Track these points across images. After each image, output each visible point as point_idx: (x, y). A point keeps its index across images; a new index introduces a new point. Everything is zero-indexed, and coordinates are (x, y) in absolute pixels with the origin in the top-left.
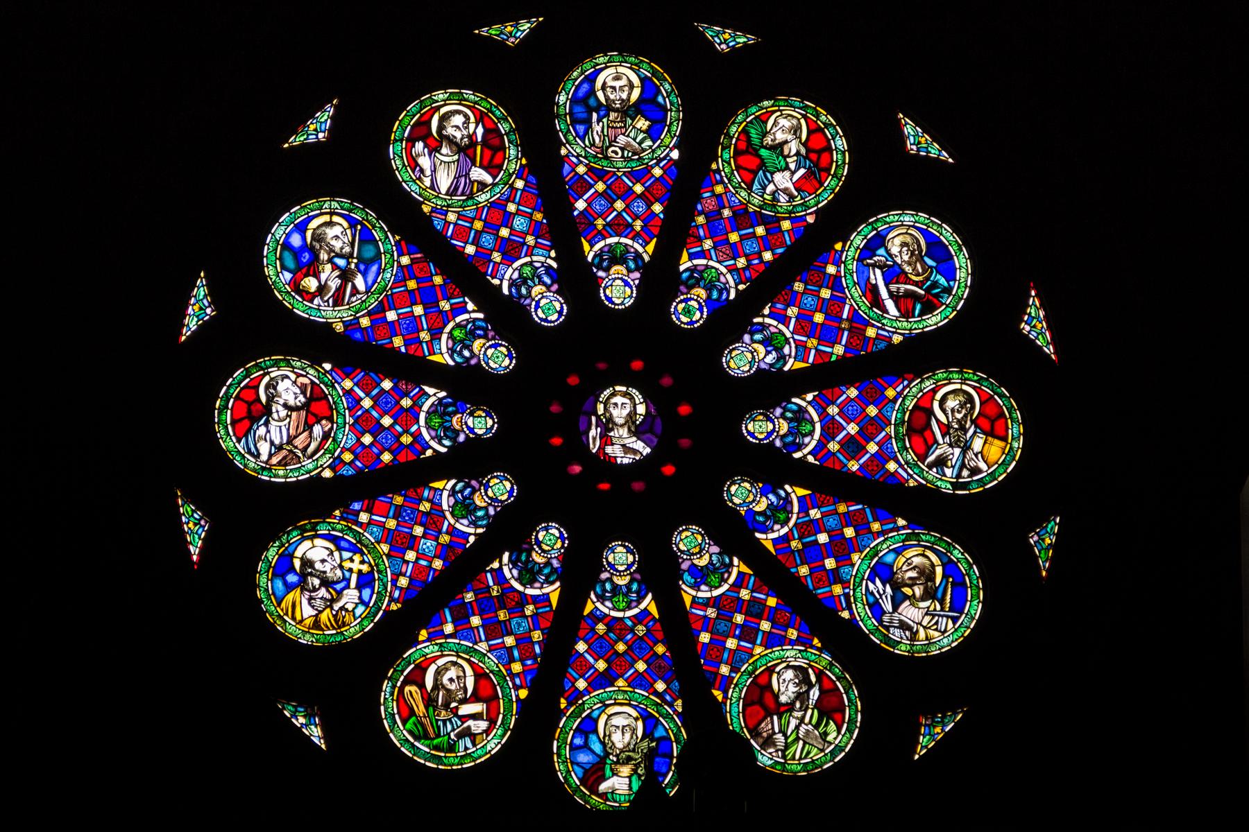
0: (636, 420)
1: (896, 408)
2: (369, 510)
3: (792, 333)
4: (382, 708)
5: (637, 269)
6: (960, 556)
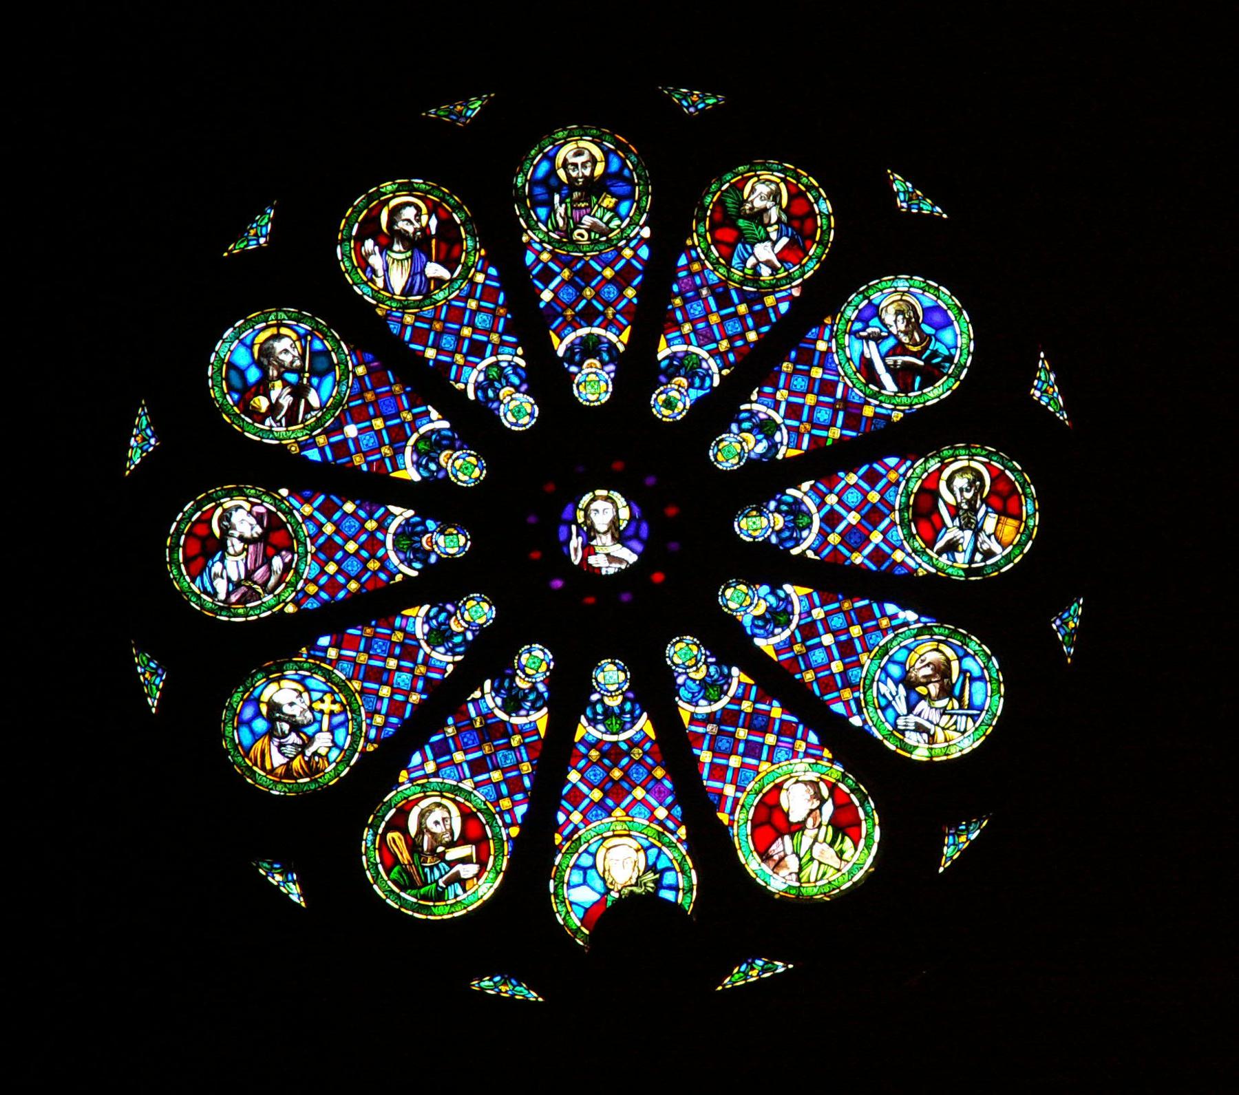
1: (900, 492)
2: (336, 644)
3: (783, 418)
4: (364, 858)
5: (611, 362)
6: (977, 648)
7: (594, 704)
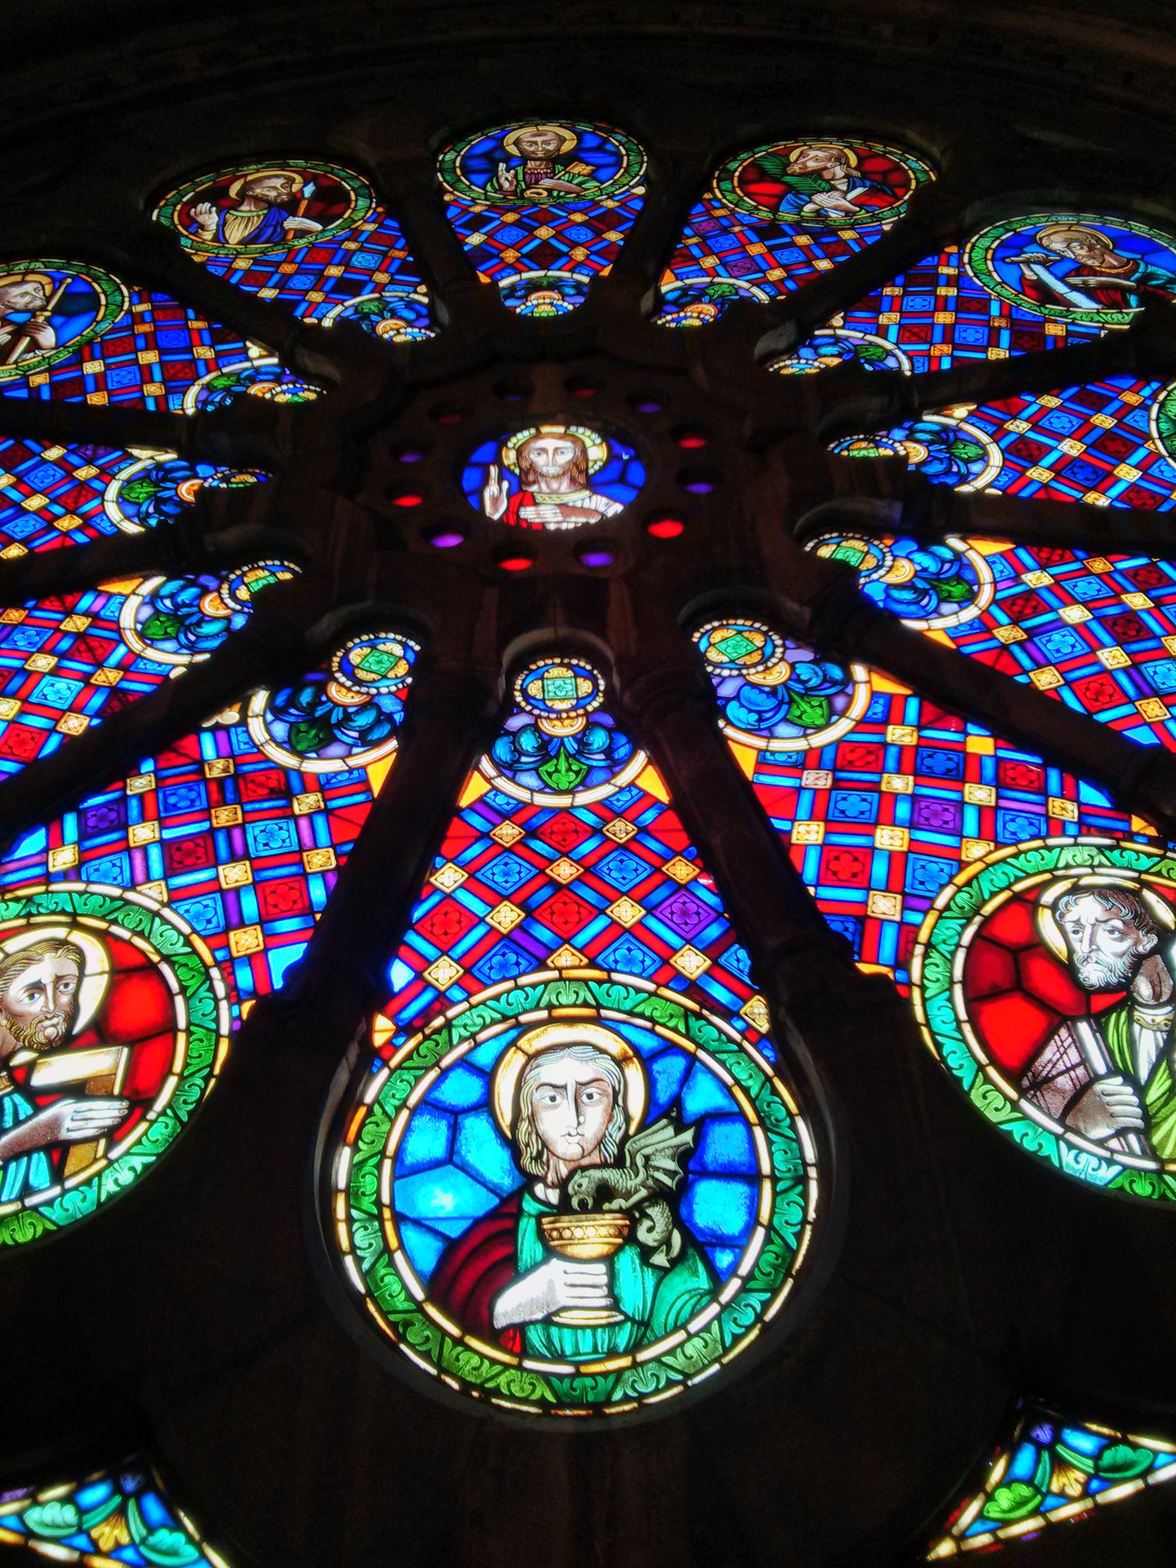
0: (587, 468)
7: (515, 735)
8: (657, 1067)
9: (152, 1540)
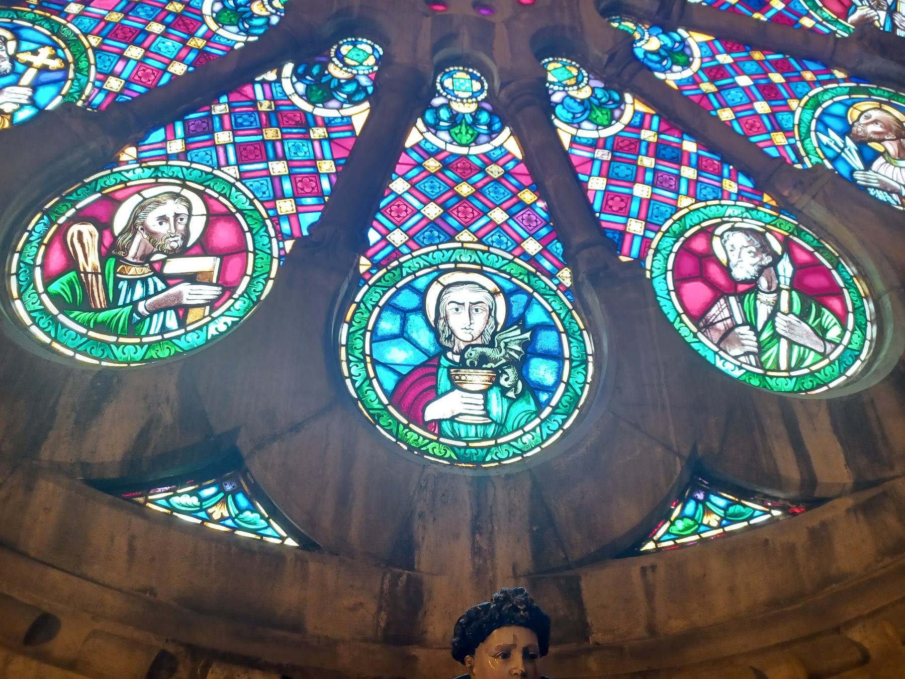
7: (437, 109)
8: (512, 299)
9: (241, 516)
